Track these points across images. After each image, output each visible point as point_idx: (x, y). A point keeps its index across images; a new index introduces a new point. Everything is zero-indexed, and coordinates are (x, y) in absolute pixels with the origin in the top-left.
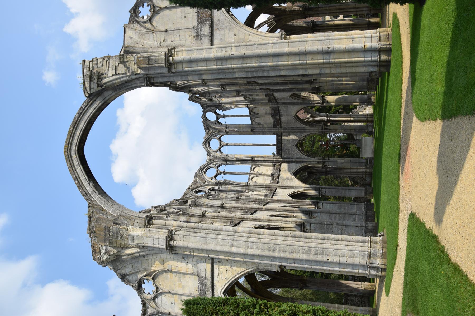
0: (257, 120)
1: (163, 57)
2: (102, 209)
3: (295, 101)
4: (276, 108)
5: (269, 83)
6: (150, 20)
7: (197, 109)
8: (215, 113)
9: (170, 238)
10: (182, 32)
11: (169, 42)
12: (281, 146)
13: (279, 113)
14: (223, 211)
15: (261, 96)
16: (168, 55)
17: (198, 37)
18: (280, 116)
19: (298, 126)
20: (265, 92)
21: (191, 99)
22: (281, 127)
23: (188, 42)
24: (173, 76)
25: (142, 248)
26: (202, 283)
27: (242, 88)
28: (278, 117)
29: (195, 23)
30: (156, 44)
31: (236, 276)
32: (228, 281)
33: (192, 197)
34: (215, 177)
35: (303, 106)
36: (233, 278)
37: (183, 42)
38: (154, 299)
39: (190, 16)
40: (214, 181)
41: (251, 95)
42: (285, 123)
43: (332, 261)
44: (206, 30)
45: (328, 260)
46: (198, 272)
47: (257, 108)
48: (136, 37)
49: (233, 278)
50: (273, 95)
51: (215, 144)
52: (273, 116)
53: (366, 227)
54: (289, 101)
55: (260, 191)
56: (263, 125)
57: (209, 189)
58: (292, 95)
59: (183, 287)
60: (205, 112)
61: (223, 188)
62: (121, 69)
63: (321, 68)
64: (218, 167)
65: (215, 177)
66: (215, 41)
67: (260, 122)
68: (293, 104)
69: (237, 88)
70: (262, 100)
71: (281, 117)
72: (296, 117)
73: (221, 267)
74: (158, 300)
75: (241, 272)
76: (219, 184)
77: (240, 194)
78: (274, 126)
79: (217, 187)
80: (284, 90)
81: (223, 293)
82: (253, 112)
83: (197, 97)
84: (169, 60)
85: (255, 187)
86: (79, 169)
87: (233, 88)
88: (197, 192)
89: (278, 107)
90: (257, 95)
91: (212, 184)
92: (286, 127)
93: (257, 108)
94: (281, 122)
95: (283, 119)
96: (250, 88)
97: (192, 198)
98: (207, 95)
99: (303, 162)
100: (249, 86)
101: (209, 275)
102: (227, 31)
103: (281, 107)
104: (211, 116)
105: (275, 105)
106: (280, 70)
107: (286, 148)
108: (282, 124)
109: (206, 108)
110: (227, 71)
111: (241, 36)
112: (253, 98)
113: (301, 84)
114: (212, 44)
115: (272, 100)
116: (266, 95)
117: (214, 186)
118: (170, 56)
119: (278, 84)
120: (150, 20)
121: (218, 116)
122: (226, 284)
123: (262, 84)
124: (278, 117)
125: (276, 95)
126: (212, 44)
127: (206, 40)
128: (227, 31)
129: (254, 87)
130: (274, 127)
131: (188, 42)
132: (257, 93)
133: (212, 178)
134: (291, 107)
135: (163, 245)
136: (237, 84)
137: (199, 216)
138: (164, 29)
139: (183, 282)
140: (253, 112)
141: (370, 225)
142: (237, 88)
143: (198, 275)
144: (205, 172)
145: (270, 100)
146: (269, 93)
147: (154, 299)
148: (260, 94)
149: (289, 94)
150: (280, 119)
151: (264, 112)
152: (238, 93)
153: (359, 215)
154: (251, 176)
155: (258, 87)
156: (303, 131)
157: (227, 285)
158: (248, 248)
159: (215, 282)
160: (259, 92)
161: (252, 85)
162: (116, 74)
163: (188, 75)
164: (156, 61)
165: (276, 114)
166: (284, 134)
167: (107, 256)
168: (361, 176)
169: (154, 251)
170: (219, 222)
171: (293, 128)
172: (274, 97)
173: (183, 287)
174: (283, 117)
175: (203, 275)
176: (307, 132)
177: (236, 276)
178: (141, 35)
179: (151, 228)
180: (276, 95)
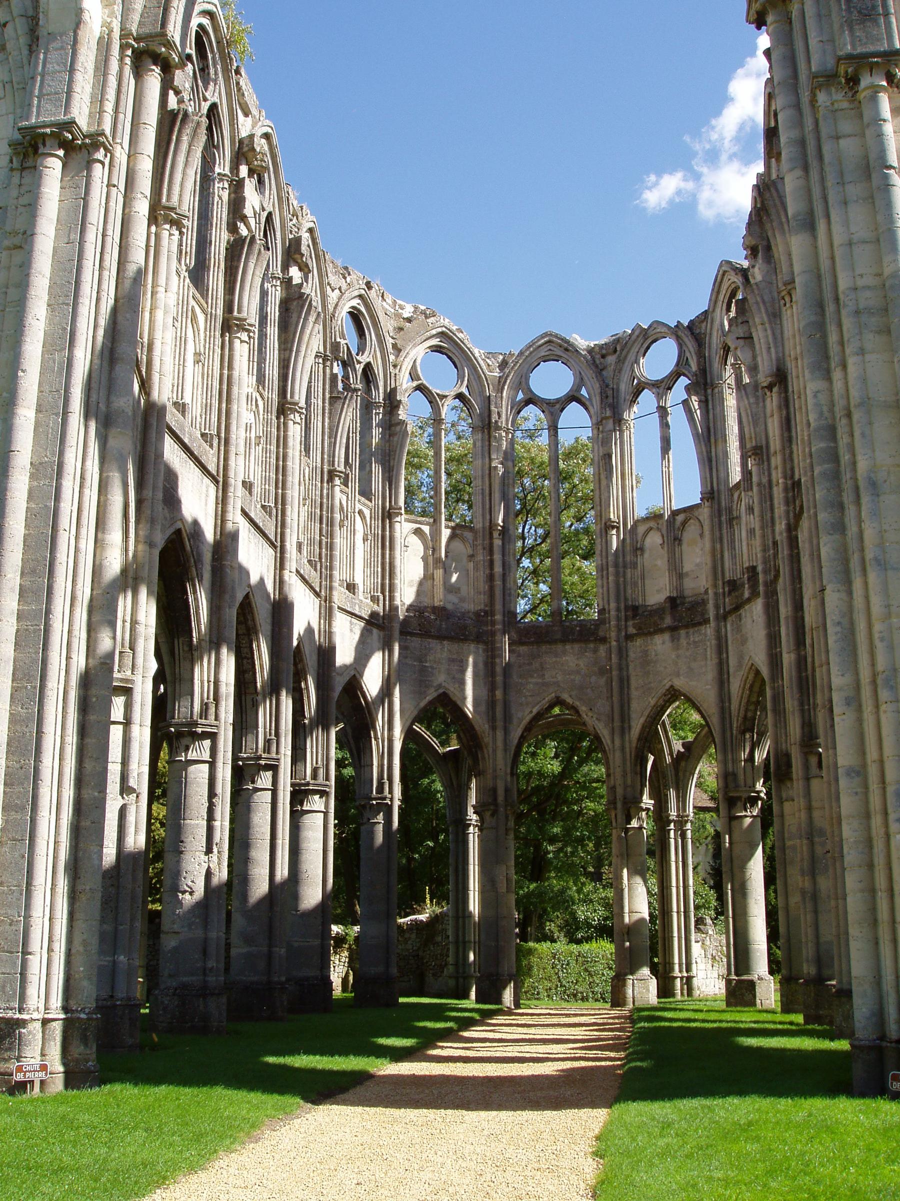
0: (654, 540)
3: (735, 686)
4: (704, 612)
5: (799, 571)
7: (690, 301)
8: (675, 375)
12: (555, 642)
13: (686, 627)
14: (267, 410)
15: (748, 549)
18: (673, 629)
19: (634, 705)
20: (765, 561)
21: (727, 267)
22: (629, 637)
24: (797, 106)
27: (776, 461)
28: (668, 621)
33: (333, 296)
34: (421, 388)
35: (715, 721)
40: (405, 383)
41: (750, 509)
42: (645, 653)
47: (702, 535)
50: (755, 594)
51: (552, 380)
52: (672, 600)
53: (204, 992)
54: (733, 662)
56: (634, 565)
57: (368, 366)
58: (758, 673)
60: (676, 332)
63: (860, 772)
64: (460, 396)
65: (421, 388)
67: (646, 555)
68: (722, 680)
69: (775, 444)
70: (734, 557)
71: (666, 636)
72: (673, 695)
76: (392, 403)
77: (355, 484)
78: (634, 611)
80: (773, 639)
82: (684, 523)
83: (733, 294)
84: (872, 67)
85: (385, 544)
87: (774, 427)
88: (355, 315)
89: (706, 621)
90: (751, 532)
92: (632, 655)
93: (702, 535)
94: (651, 634)
95: (660, 644)
96: (778, 494)
97: (324, 297)
98: (740, 331)
99: (494, 728)
100: (786, 490)
103: (709, 631)
104: (659, 360)
105: (717, 607)
106: (848, 583)
107: (549, 660)
108: (639, 642)
109: (693, 334)
110: (833, 338)
112: (738, 518)
113: (801, 704)
115: (734, 593)
116: (753, 569)
117: (381, 384)
119: (798, 606)
121: (663, 386)
123: (793, 542)
124: (668, 621)
125: (756, 610)
129: (780, 509)
130: (627, 608)
132: (758, 533)
133: (414, 376)
134: (710, 674)
136: (790, 440)
140: (684, 523)
141: (216, 1008)
142: (775, 444)
144: (437, 349)
145: (733, 586)
146: (761, 577)
148: (757, 542)
149: (760, 659)
150: (661, 631)
151: (687, 567)
152: (754, 451)
153: (270, 956)
155: (781, 526)
156: (617, 724)
160: (763, 536)
161: (787, 503)
163: (806, 168)
165: (682, 613)
166: (602, 649)
168: (451, 960)
170: (208, 389)
171: (624, 682)
172: (749, 600)
174: (668, 644)
176: (613, 742)
180: (756, 610)
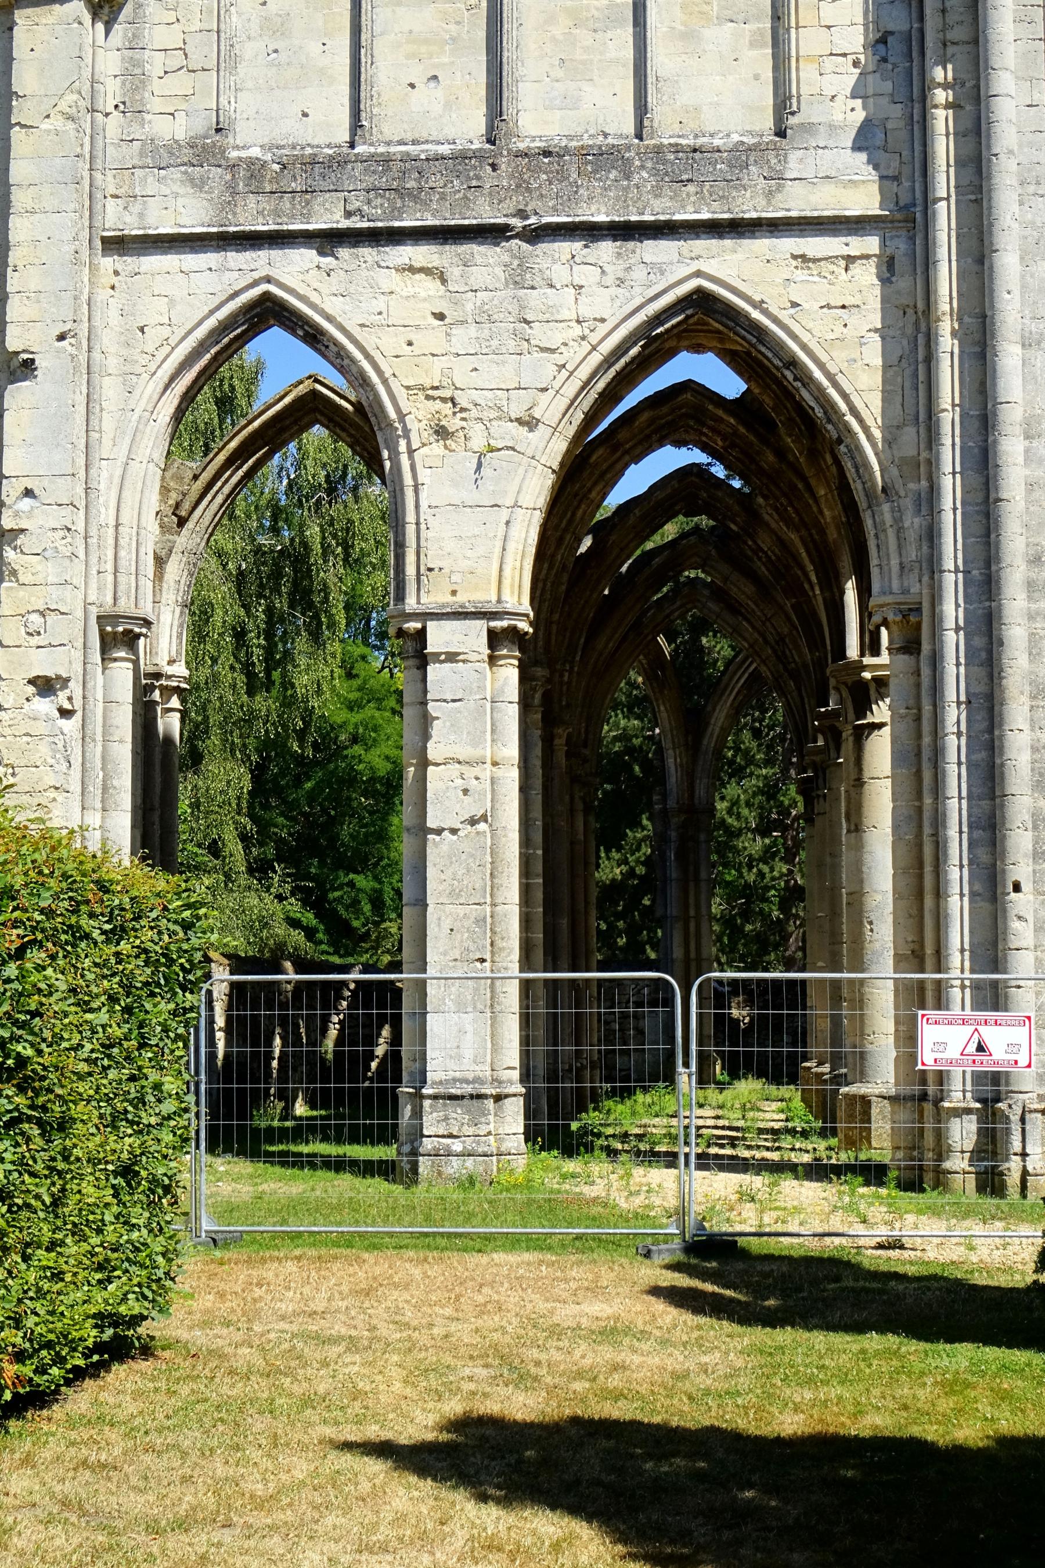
26: (742, 156)
31: (821, 366)
32: (784, 316)
36: (804, 347)
43: (1012, 913)
45: (1017, 888)
46: (808, 128)
49: (804, 347)
59: (689, 36)
73: (867, 275)
75: (845, 396)
81: (699, 291)
101: (796, 202)
122: (758, 305)
139: (720, 37)
157: (755, 314)
158: (1027, 437)
159: (762, 245)
173: (689, 36)
175: (795, 164)
177: (821, 366)
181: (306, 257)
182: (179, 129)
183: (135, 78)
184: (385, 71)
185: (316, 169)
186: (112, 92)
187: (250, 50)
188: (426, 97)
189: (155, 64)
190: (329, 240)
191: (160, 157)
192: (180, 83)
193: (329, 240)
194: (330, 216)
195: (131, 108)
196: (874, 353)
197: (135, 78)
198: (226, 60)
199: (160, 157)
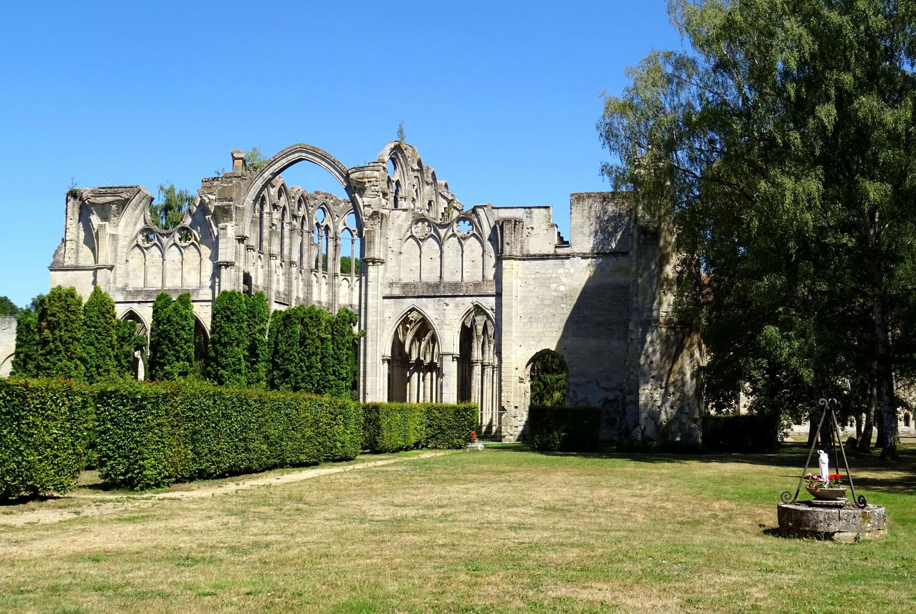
1: (372, 256)
2: (248, 190)
6: (412, 236)
9: (228, 265)
10: (397, 268)
11: (390, 256)
16: (374, 261)
17: (391, 284)
23: (388, 275)
25: (217, 238)
26: (194, 290)
29: (405, 281)
30: (390, 243)
37: (389, 270)
38: (175, 244)
39: (412, 275)
44: (397, 292)
48: (399, 222)
55: (328, 293)
61: (331, 243)
62: (368, 211)
66: (386, 300)
73: (210, 308)
74: (174, 247)
79: (331, 234)
86: (284, 162)
91: (335, 227)
102: (393, 310)
111: (388, 323)
114: (384, 298)
118: (373, 263)
120: (412, 236)
126: (384, 298)
127: (387, 292)
128: (393, 310)
131: (388, 275)
135: (221, 258)
137: (270, 250)
138: (403, 250)
143: (201, 287)
147: (175, 244)
154: (349, 278)
162: (364, 206)
164: (369, 249)
167: (207, 201)
169: (215, 247)
178: (400, 227)
179: (235, 243)
181: (136, 304)
182: (120, 285)
183: (115, 278)
184: (149, 277)
185: (138, 292)
186: (112, 280)
187: (131, 274)
188: (154, 281)
189: (118, 276)
190: (139, 302)
191: (118, 290)
192: (121, 279)
193: (139, 302)
194: (140, 299)
195: (115, 283)
196: (210, 319)
197: (115, 278)
198: (128, 275)
199: (118, 290)
